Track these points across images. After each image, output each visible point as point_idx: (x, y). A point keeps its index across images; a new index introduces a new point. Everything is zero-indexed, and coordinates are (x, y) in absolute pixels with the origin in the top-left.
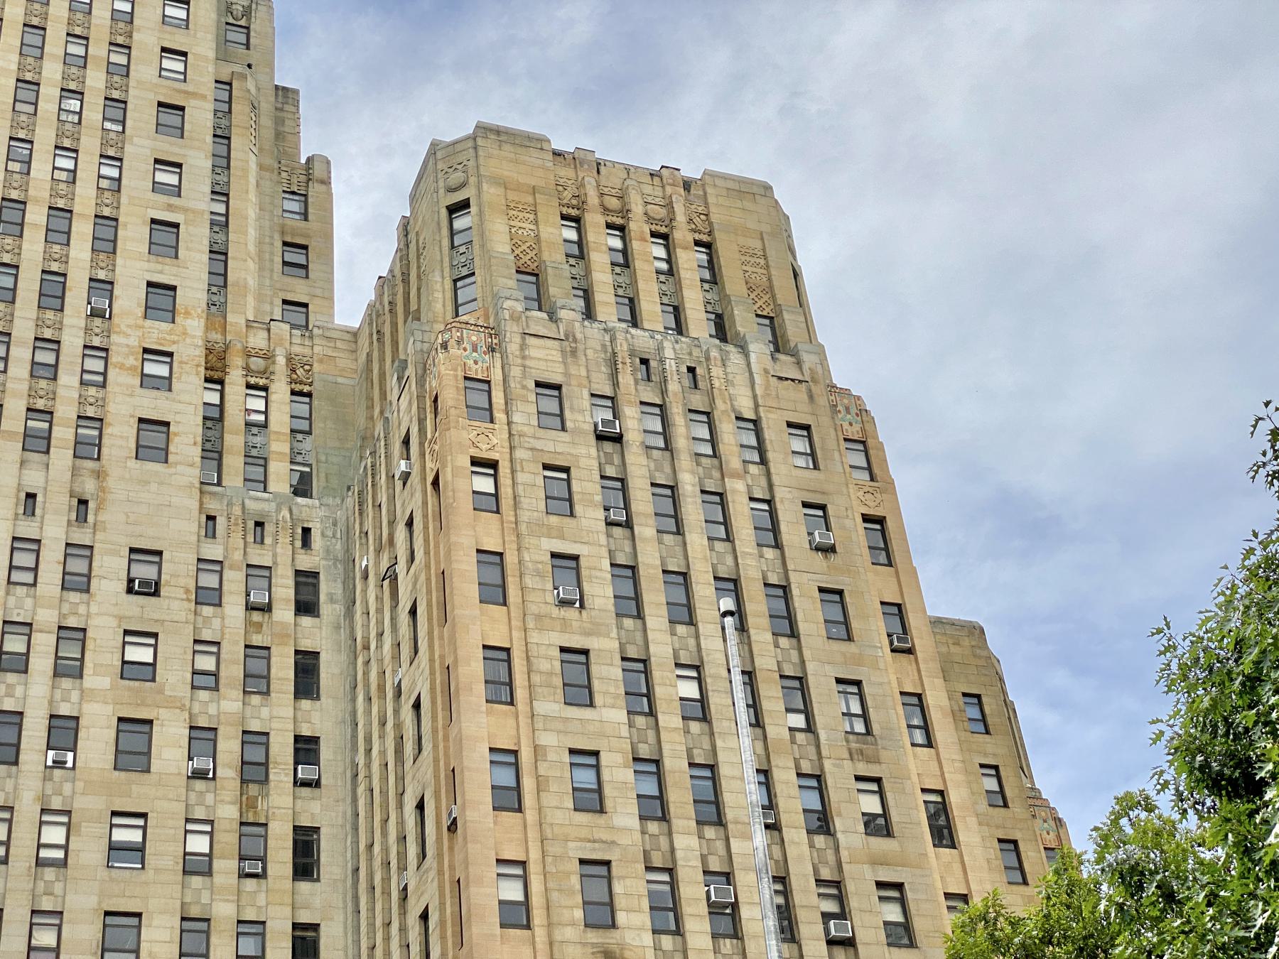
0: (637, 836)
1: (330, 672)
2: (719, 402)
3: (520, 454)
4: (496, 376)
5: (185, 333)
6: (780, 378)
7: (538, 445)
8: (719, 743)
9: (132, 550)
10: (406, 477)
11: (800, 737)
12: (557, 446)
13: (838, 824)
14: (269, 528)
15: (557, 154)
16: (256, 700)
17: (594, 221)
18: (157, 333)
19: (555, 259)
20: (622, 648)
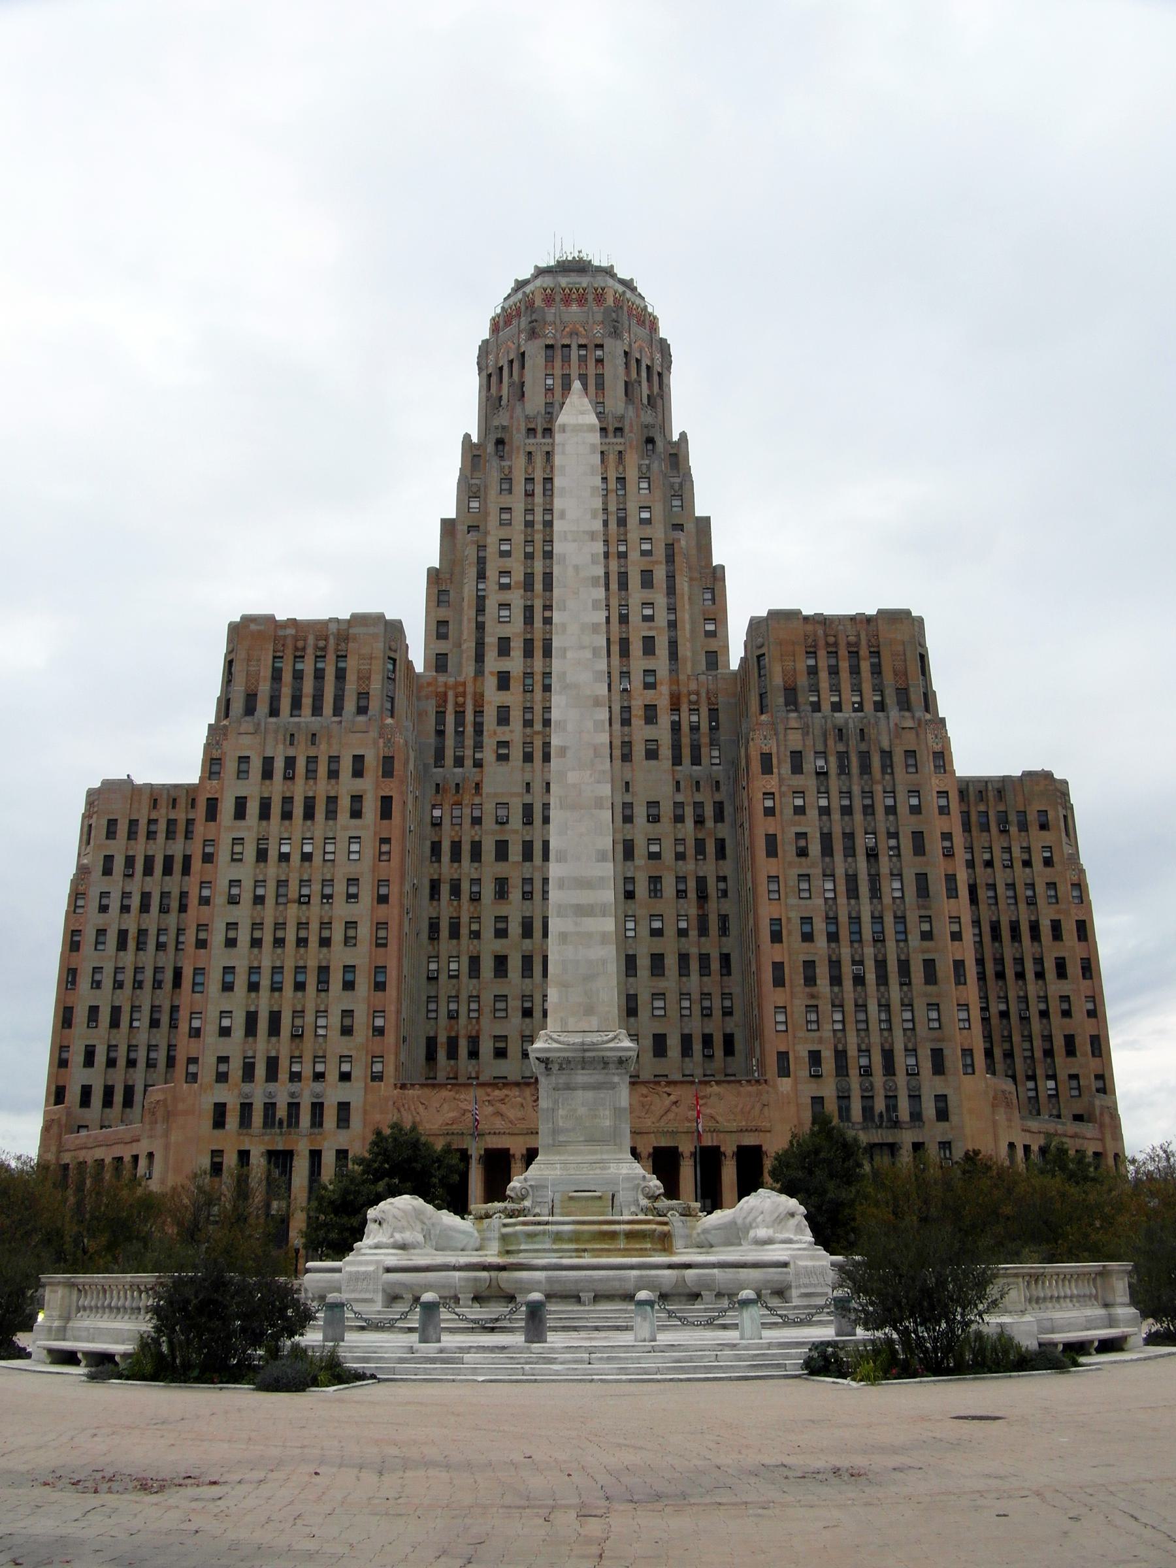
0: (826, 950)
2: (872, 747)
3: (784, 789)
4: (774, 751)
6: (903, 728)
8: (862, 908)
11: (898, 901)
13: (910, 937)
15: (806, 619)
16: (701, 862)
17: (822, 653)
18: (649, 696)
19: (803, 681)
20: (824, 870)
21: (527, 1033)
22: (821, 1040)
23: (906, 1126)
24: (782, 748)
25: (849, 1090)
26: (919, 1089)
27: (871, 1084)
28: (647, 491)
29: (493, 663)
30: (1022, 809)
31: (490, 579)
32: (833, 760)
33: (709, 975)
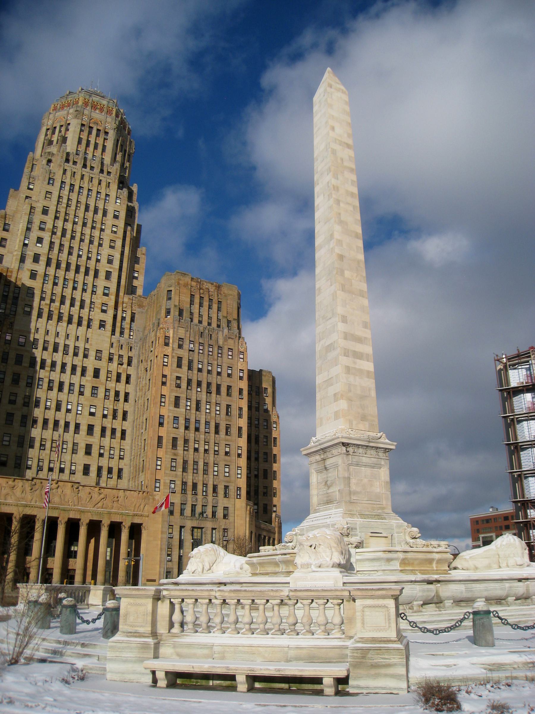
1: (133, 379)
4: (171, 336)
5: (111, 300)
7: (177, 352)
9: (97, 350)
10: (151, 351)
12: (180, 352)
14: (123, 346)
21: (19, 455)
22: (176, 476)
23: (209, 520)
24: (175, 335)
25: (186, 501)
26: (217, 503)
27: (197, 499)
28: (119, 204)
29: (29, 264)
30: (258, 386)
31: (35, 223)
32: (197, 345)
33: (115, 439)
